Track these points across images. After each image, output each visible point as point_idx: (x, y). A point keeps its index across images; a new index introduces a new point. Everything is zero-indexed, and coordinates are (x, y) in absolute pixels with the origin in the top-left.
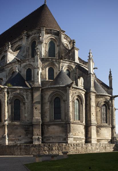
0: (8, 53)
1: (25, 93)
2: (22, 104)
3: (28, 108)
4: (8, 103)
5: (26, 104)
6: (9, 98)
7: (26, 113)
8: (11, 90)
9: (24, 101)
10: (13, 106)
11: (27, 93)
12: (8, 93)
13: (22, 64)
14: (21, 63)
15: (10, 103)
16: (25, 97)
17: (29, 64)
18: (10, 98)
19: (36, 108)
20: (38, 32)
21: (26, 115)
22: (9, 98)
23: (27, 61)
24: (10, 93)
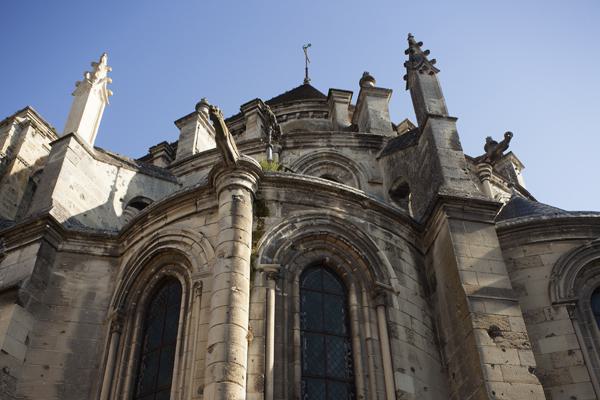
0: (198, 123)
1: (379, 234)
2: (360, 299)
3: (410, 331)
4: (260, 277)
5: (395, 298)
6: (266, 240)
7: (402, 371)
8: (283, 192)
9: (382, 279)
10: (292, 298)
11: (391, 237)
12: (260, 209)
13: (286, 153)
14: (284, 148)
15: (277, 277)
16: (383, 255)
17: (331, 156)
18: (279, 242)
19: (494, 332)
20: (314, 112)
21: (406, 383)
22: (266, 240)
23: (320, 143)
24: (276, 211)
